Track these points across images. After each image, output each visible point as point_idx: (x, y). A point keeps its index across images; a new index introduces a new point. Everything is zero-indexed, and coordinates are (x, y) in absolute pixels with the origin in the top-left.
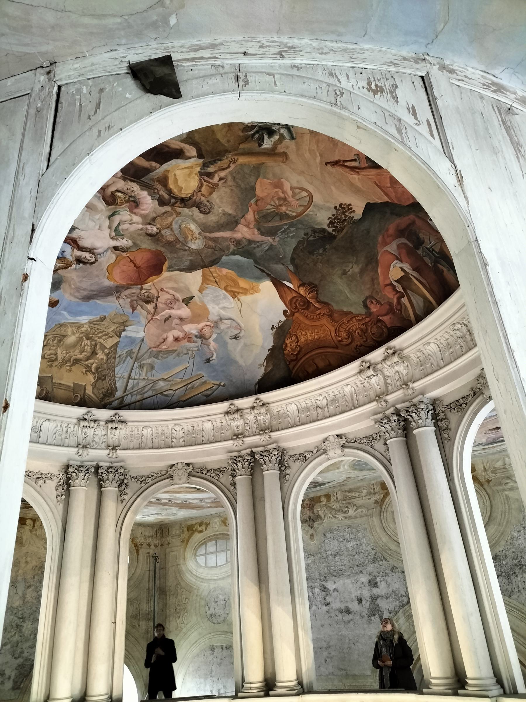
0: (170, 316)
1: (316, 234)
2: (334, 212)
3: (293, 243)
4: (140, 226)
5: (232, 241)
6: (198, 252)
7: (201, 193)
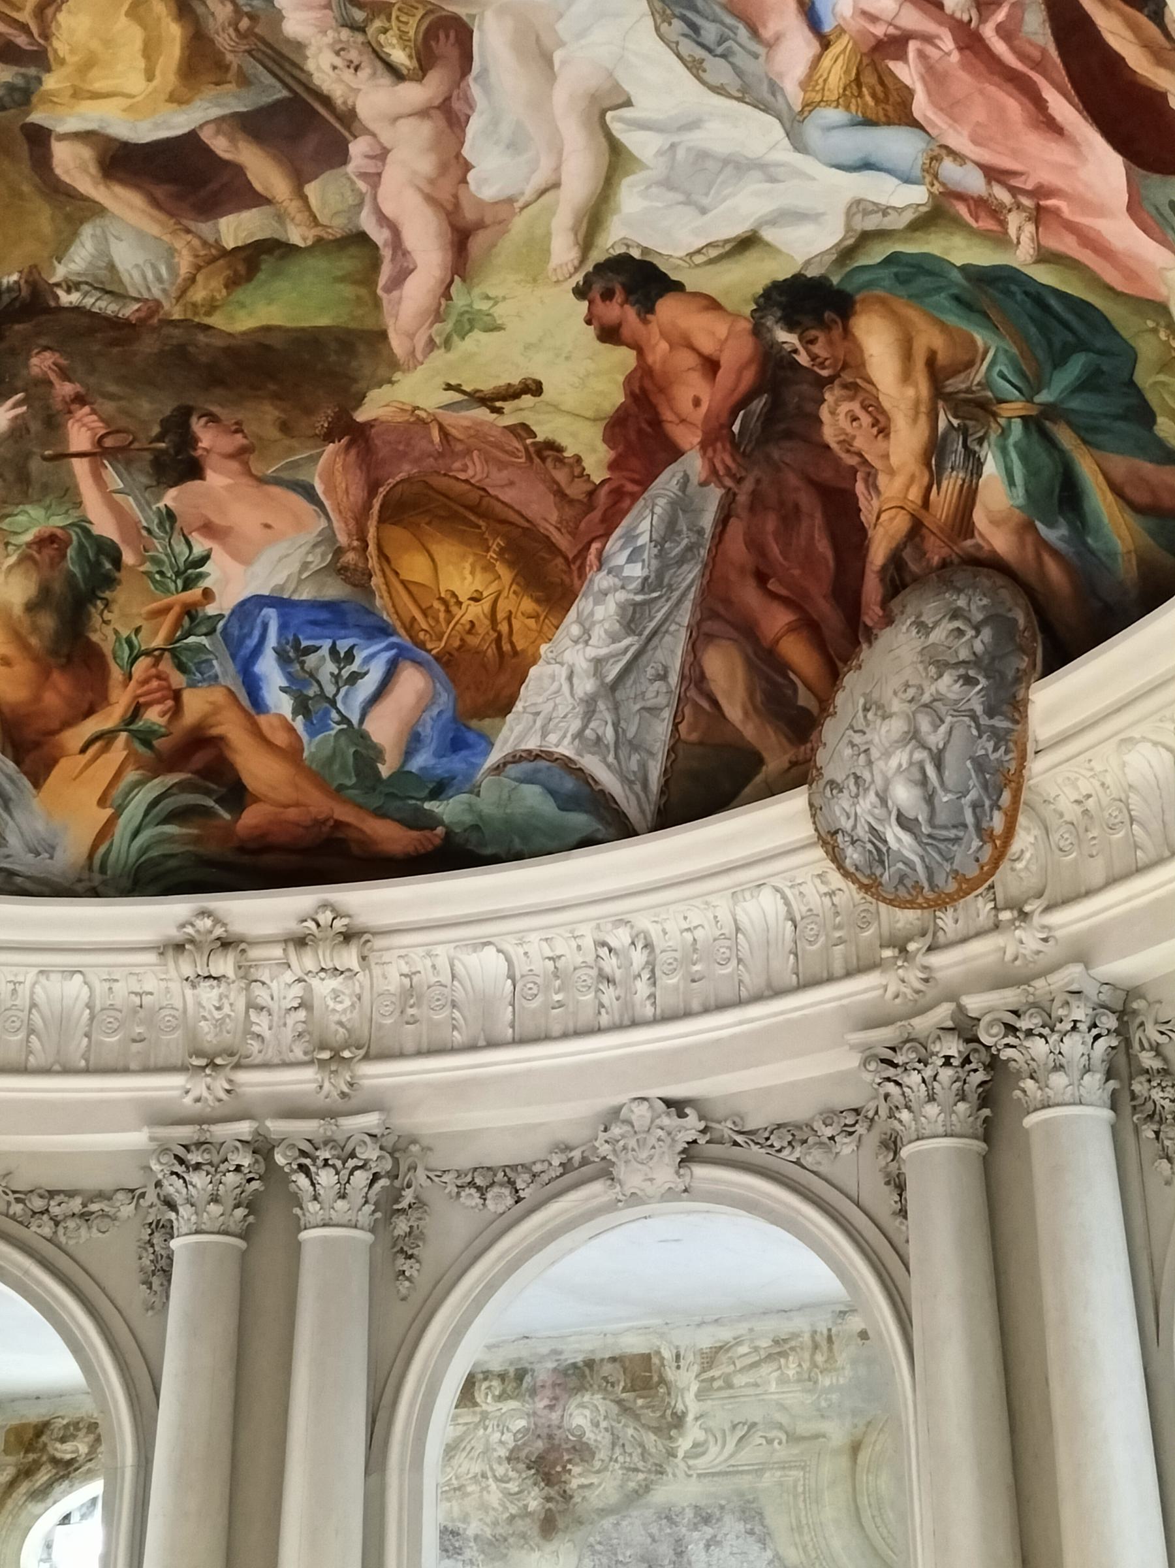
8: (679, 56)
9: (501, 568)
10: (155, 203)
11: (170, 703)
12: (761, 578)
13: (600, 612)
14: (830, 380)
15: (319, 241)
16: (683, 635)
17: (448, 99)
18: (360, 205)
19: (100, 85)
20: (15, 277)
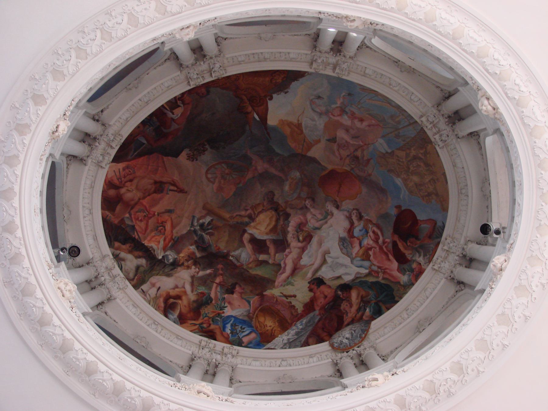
0: (353, 137)
4: (312, 210)
8: (340, 247)
9: (276, 323)
10: (253, 248)
11: (208, 325)
12: (323, 329)
13: (292, 332)
14: (345, 300)
16: (306, 336)
17: (304, 247)
18: (283, 259)
19: (258, 227)
20: (226, 251)
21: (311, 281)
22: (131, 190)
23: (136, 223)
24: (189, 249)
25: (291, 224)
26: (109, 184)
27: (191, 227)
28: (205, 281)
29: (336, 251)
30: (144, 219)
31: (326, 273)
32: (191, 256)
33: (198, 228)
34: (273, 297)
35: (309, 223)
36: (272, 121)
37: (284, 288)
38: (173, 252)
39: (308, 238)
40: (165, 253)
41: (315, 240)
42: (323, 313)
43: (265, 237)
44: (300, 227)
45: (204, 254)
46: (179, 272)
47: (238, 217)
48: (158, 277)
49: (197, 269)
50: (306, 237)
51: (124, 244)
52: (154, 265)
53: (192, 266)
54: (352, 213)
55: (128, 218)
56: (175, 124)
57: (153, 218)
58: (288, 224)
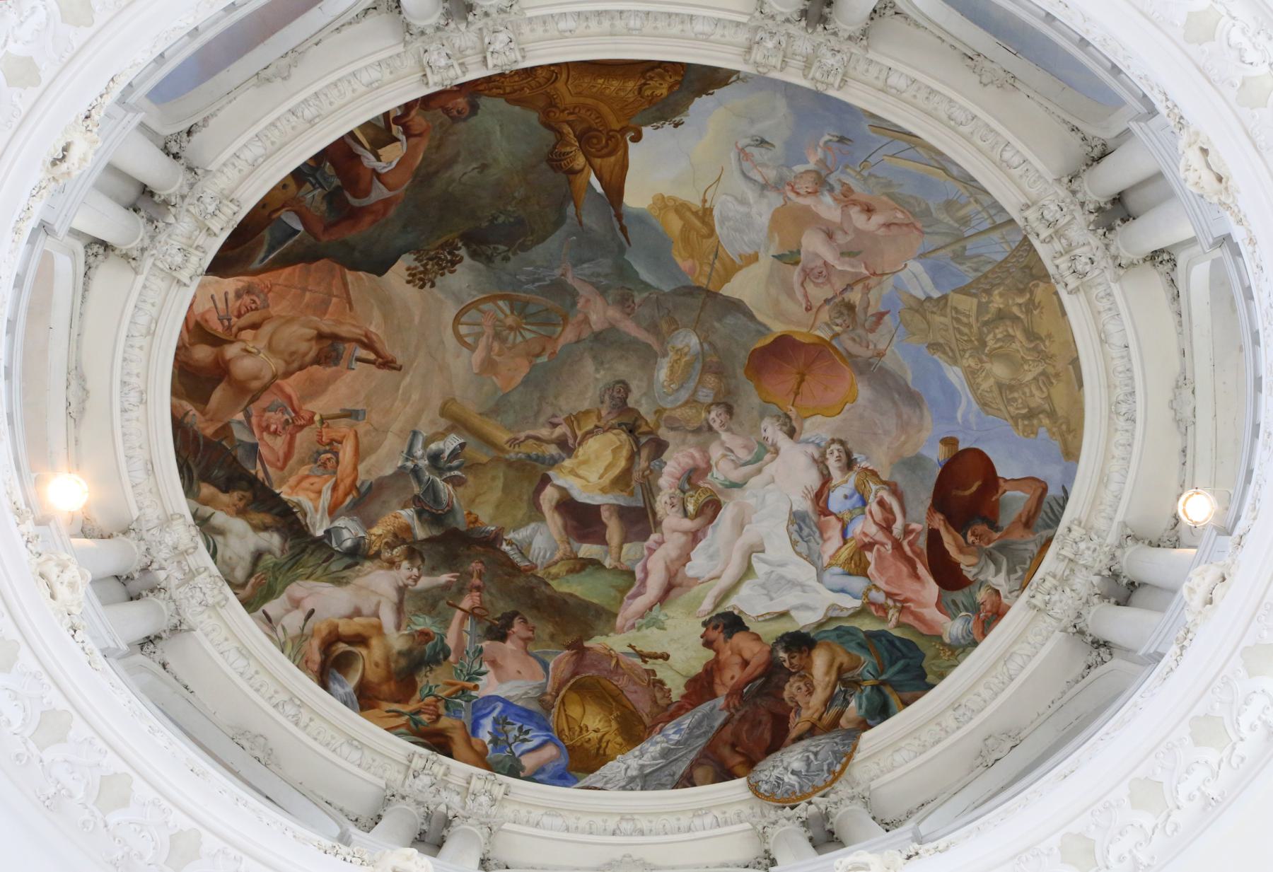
0: (842, 254)
1: (489, 252)
2: (438, 280)
3: (539, 252)
4: (725, 436)
5: (628, 310)
6: (697, 326)
7: (598, 424)
10: (565, 527)
12: (733, 746)
13: (652, 749)
14: (795, 673)
15: (615, 568)
18: (639, 560)
19: (581, 472)
20: (493, 528)
21: (710, 620)
22: (253, 350)
23: (262, 439)
24: (396, 517)
25: (666, 469)
26: (196, 331)
27: (407, 460)
28: (433, 602)
29: (779, 546)
30: (284, 428)
31: (749, 602)
32: (401, 536)
33: (424, 463)
34: (609, 655)
35: (714, 470)
36: (636, 197)
37: (639, 634)
38: (353, 520)
39: (711, 508)
40: (332, 521)
41: (727, 515)
42: (735, 705)
43: (595, 498)
44: (692, 477)
45: (436, 532)
46: (366, 575)
47: (531, 442)
48: (310, 583)
49: (415, 571)
50: (706, 504)
51: (226, 491)
52: (303, 551)
53: (401, 561)
54: (828, 451)
55: (240, 422)
56: (381, 186)
57: (307, 430)
58: (661, 468)
